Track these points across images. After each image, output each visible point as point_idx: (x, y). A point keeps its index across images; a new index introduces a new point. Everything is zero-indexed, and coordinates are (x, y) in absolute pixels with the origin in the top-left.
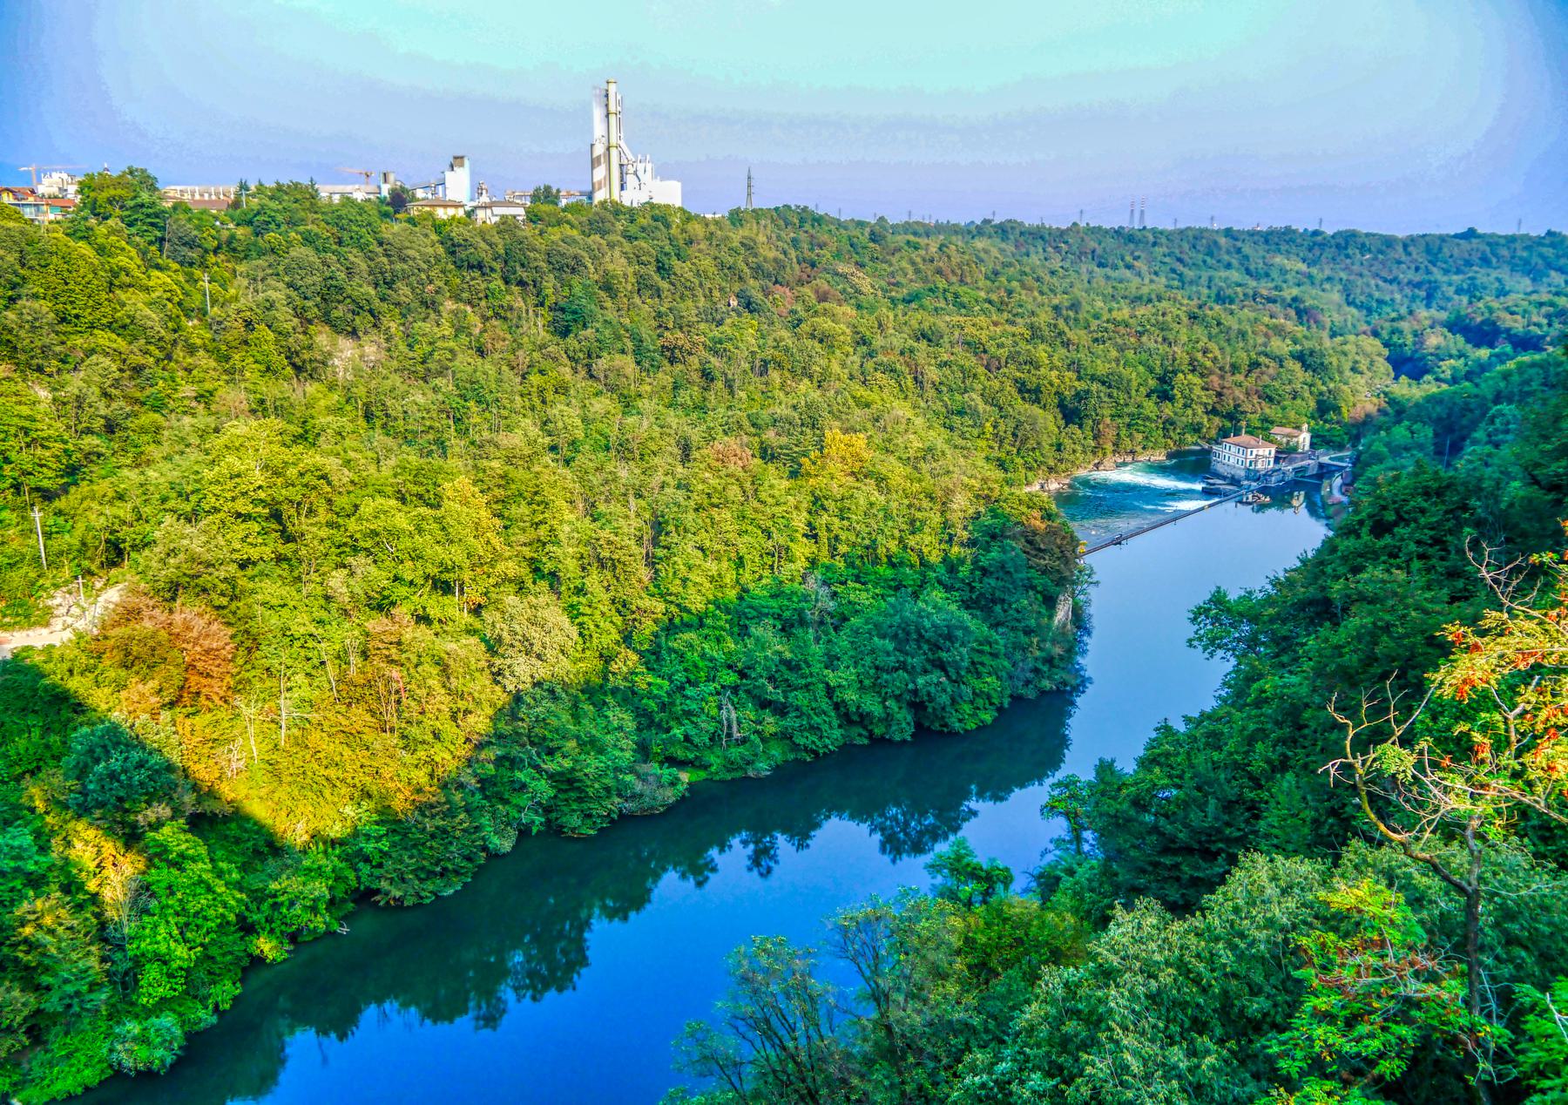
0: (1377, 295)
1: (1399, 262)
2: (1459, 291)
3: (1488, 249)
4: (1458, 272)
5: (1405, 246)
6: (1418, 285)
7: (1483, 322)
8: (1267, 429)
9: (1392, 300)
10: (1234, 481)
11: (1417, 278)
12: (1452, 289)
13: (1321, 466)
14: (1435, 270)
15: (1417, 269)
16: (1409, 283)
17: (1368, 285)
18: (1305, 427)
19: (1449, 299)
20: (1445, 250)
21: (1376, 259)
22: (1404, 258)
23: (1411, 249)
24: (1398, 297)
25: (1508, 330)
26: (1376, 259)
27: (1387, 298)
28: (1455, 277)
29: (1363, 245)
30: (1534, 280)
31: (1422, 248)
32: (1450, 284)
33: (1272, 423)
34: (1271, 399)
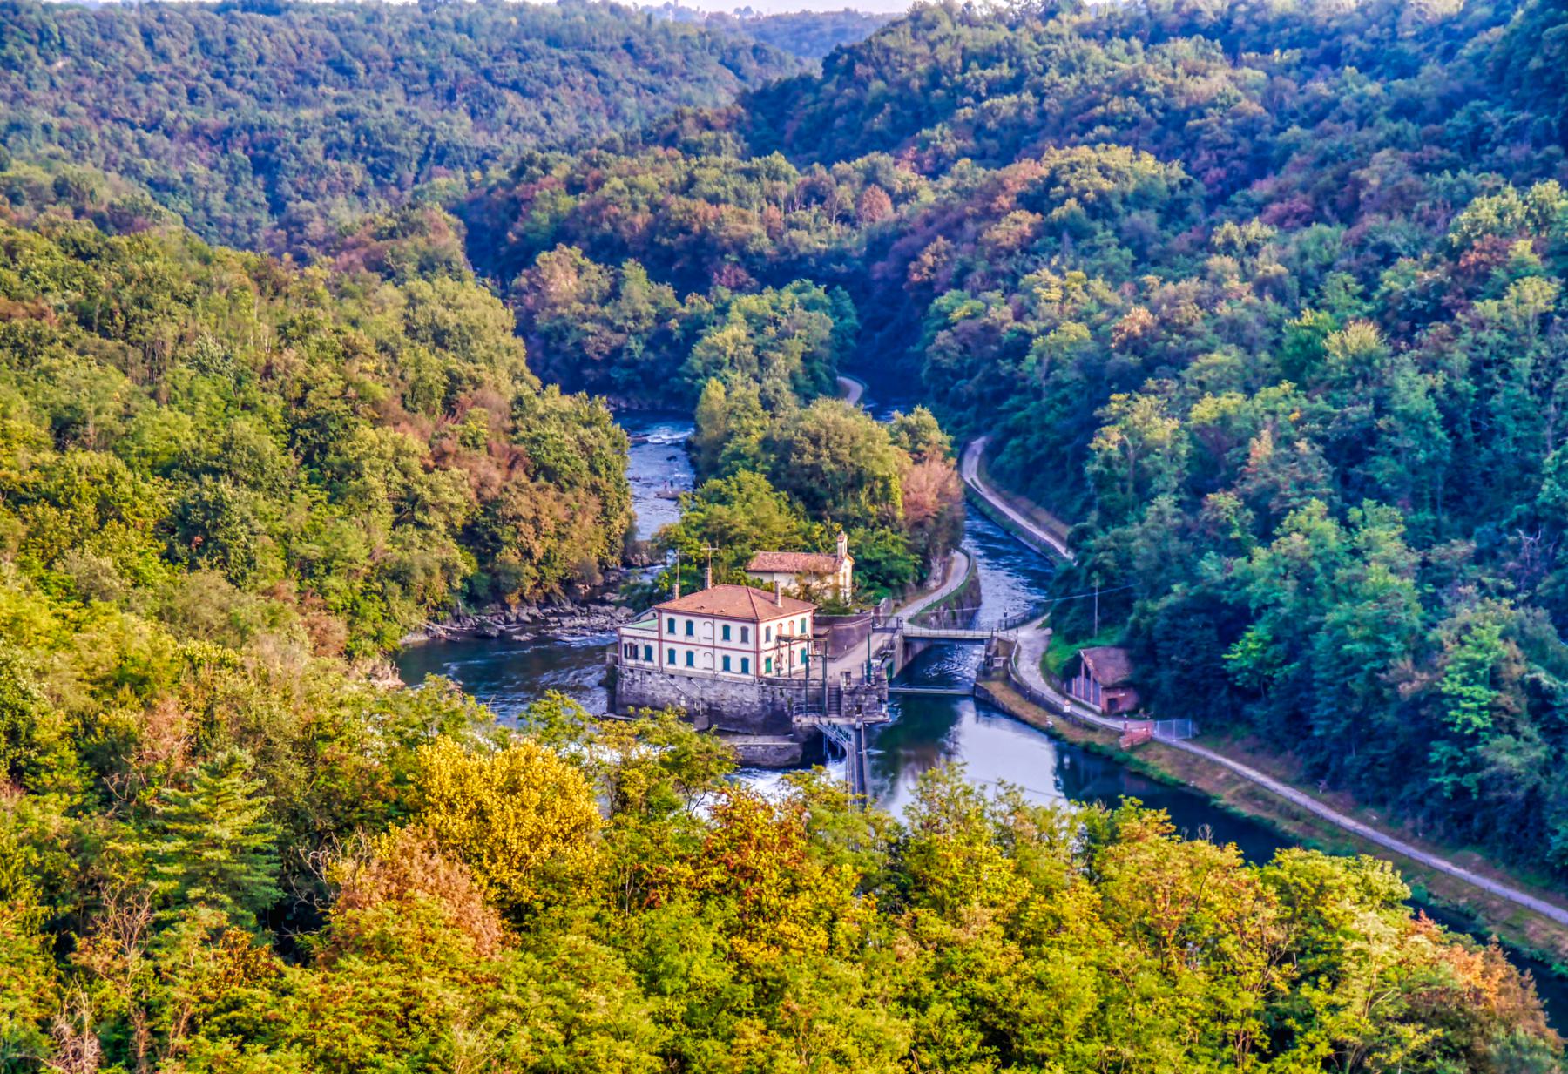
0: (149, 167)
1: (145, 78)
2: (334, 149)
3: (334, 38)
4: (295, 102)
5: (148, 37)
6: (224, 138)
7: (652, 229)
8: (742, 561)
9: (188, 179)
10: (719, 720)
11: (215, 119)
12: (315, 145)
13: (908, 642)
14: (234, 95)
15: (192, 94)
16: (196, 132)
17: (120, 144)
18: (843, 543)
19: (314, 171)
20: (243, 43)
21: (82, 69)
22: (151, 68)
23: (163, 41)
24: (197, 169)
25: (739, 246)
26: (82, 69)
27: (176, 175)
28: (305, 114)
29: (44, 34)
30: (473, 114)
31: (188, 40)
32: (303, 134)
33: (743, 538)
34: (550, 474)
